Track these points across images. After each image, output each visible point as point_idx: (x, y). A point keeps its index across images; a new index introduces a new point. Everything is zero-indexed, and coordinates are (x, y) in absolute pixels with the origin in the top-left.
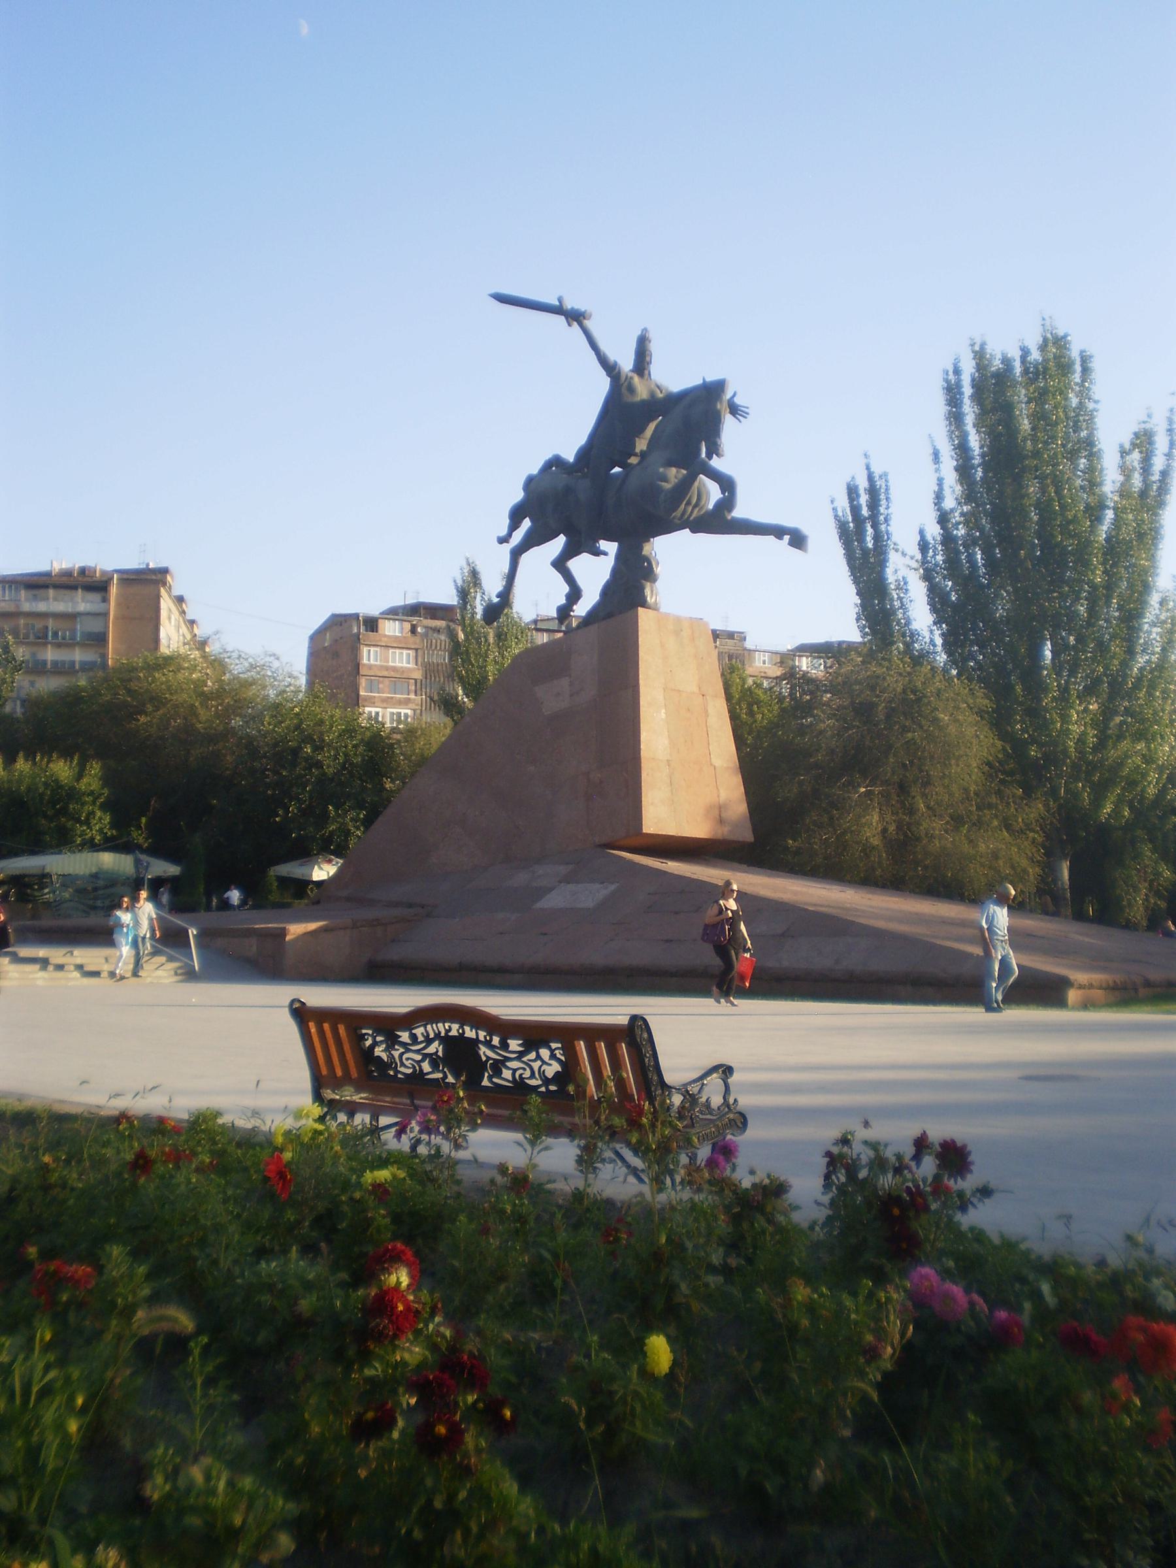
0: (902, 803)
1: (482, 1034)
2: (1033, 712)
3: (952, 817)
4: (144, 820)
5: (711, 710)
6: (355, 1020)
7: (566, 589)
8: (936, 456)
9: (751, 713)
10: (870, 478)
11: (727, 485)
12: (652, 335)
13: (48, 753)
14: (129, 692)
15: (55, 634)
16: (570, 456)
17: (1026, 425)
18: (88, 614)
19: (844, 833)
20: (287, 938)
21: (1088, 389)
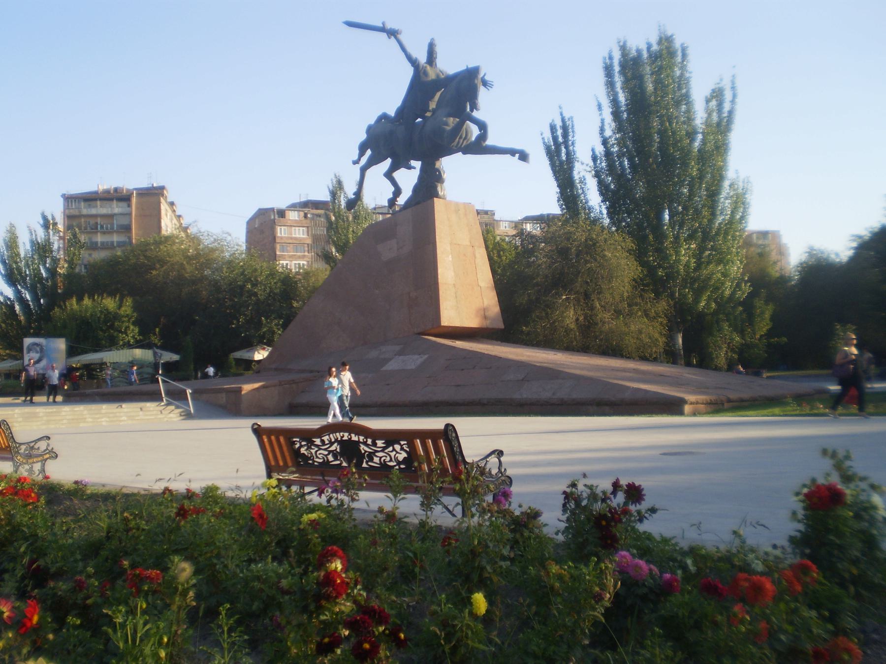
0: (587, 304)
1: (361, 438)
2: (659, 250)
3: (615, 311)
4: (157, 330)
5: (478, 255)
6: (289, 434)
7: (393, 189)
8: (600, 107)
9: (499, 256)
10: (563, 120)
11: (482, 126)
12: (437, 42)
13: (101, 294)
14: (145, 256)
15: (102, 227)
16: (392, 113)
17: (650, 87)
19: (554, 322)
20: (243, 393)
21: (686, 66)
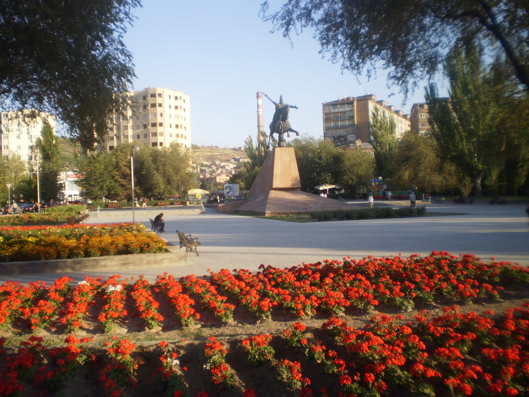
12: (283, 96)
15: (341, 118)
18: (349, 111)
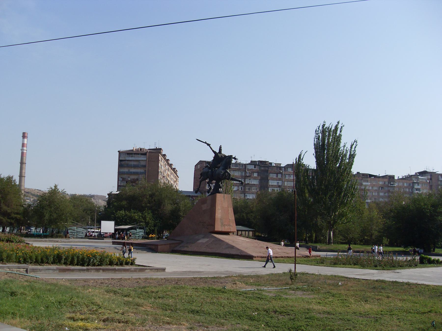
5: (230, 210)
